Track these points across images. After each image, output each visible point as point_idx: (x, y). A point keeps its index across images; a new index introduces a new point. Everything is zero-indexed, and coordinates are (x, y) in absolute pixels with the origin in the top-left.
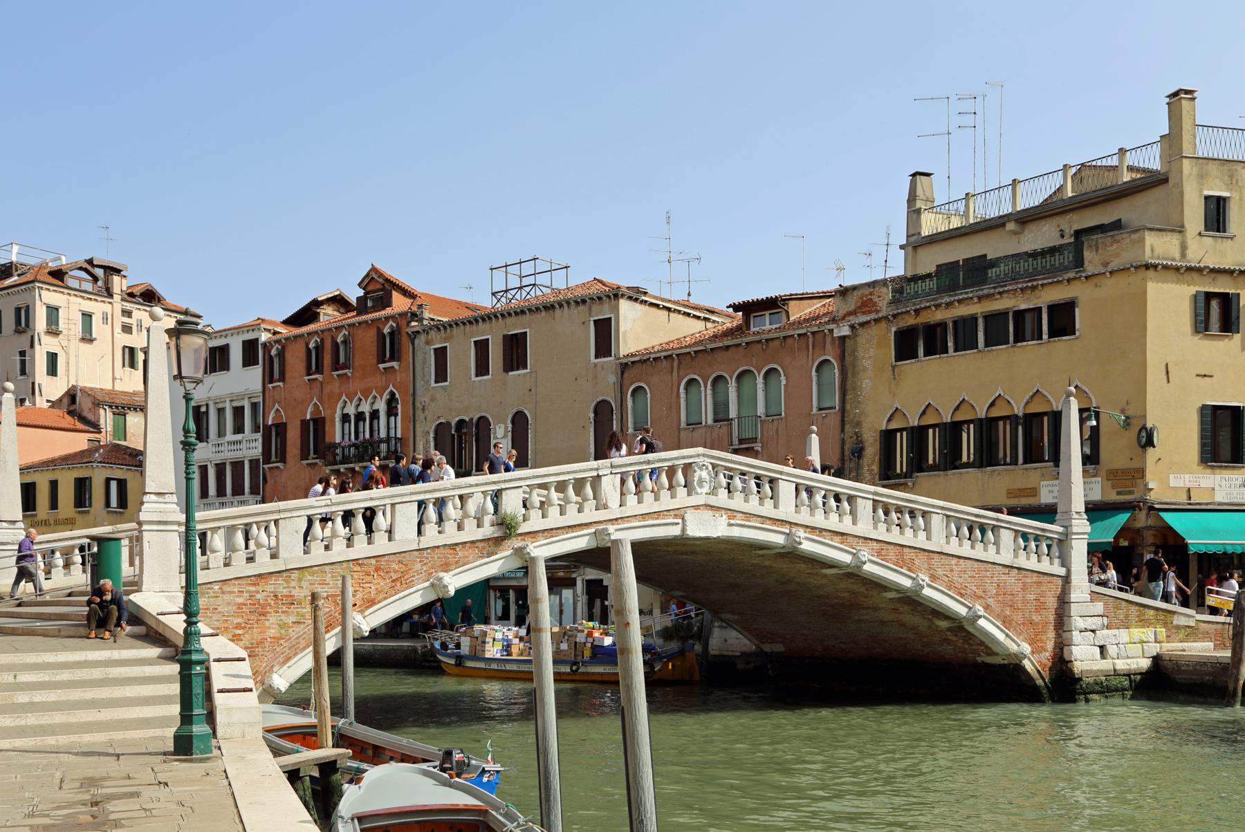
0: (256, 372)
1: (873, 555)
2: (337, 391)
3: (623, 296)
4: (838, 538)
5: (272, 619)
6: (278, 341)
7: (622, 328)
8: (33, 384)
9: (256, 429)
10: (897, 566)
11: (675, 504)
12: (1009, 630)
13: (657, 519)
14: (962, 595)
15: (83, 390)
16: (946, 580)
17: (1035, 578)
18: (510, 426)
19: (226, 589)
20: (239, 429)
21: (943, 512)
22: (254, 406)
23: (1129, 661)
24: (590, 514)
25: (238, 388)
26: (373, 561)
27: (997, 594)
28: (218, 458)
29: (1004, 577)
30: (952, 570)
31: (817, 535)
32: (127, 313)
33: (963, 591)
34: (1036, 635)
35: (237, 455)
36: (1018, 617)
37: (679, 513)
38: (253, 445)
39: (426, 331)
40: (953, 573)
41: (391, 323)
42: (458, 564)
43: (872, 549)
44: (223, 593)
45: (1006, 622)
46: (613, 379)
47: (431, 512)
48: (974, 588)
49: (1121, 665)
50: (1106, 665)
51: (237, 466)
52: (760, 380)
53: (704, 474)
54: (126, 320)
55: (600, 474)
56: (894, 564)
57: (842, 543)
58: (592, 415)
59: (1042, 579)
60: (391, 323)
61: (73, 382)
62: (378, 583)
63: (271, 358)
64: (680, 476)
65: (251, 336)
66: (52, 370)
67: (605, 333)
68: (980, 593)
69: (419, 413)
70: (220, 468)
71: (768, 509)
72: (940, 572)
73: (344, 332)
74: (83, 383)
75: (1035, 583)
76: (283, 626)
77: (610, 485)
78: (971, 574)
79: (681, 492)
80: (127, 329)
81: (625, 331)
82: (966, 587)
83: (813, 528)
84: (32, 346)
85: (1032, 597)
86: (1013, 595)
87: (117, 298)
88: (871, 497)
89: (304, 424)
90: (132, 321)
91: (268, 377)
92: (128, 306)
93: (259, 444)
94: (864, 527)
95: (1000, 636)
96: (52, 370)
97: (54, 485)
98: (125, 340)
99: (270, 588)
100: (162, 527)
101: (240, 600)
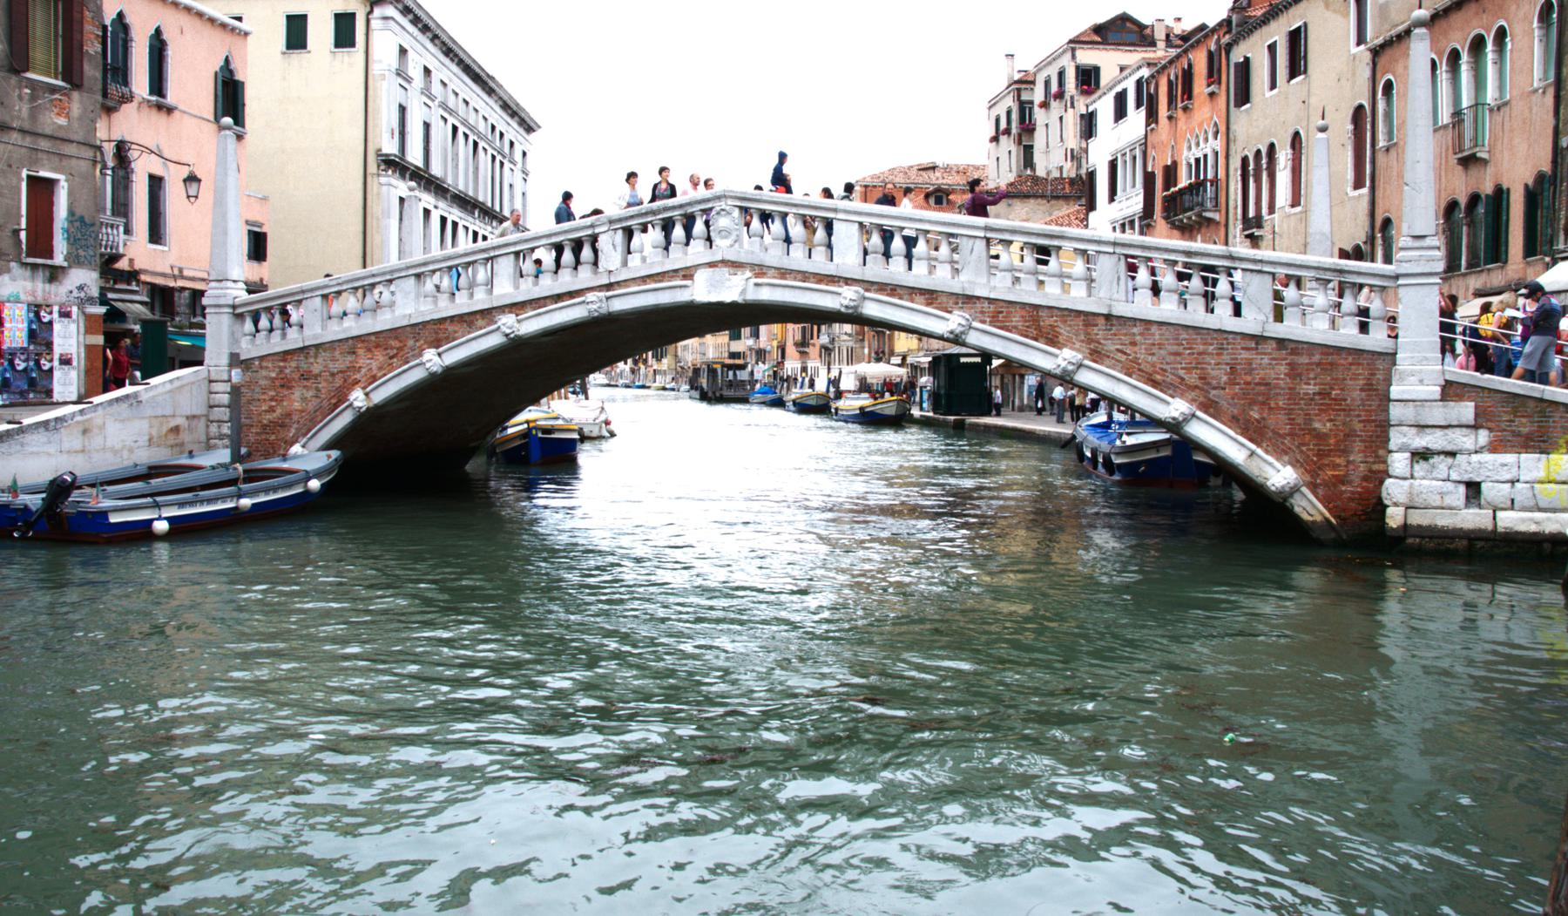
1: (983, 322)
4: (918, 298)
5: (297, 393)
10: (1027, 336)
12: (1259, 445)
13: (660, 281)
14: (1155, 384)
16: (1123, 358)
19: (264, 364)
21: (1119, 250)
23: (1538, 515)
24: (585, 277)
26: (373, 338)
27: (1232, 383)
29: (1245, 355)
30: (1134, 344)
31: (888, 295)
33: (1158, 377)
34: (1321, 454)
36: (1279, 421)
37: (687, 273)
40: (1136, 349)
42: (449, 339)
43: (982, 312)
44: (261, 368)
45: (1253, 432)
48: (1182, 373)
49: (1510, 520)
50: (1473, 519)
55: (597, 231)
56: (1022, 335)
57: (928, 304)
62: (368, 361)
64: (699, 227)
68: (1192, 379)
71: (819, 263)
72: (1110, 346)
75: (1318, 364)
76: (304, 399)
78: (1175, 348)
82: (1165, 370)
85: (1312, 389)
86: (1267, 384)
88: (981, 234)
99: (294, 364)
100: (217, 310)
101: (273, 375)
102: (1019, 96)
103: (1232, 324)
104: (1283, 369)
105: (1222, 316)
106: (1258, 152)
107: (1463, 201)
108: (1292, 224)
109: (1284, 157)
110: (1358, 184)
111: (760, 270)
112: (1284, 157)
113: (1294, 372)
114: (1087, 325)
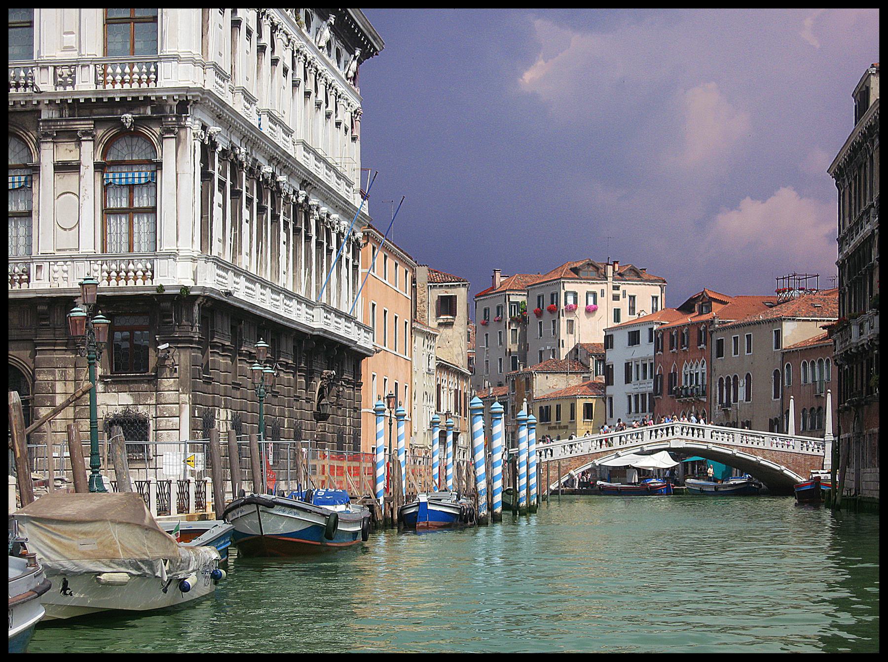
0: (653, 345)
2: (683, 359)
3: (784, 319)
6: (660, 330)
7: (784, 336)
8: (559, 340)
9: (651, 377)
11: (668, 438)
15: (582, 346)
17: (810, 457)
18: (745, 380)
20: (645, 378)
22: (651, 364)
24: (640, 442)
25: (644, 355)
27: (793, 462)
28: (635, 392)
32: (616, 288)
35: (644, 390)
37: (668, 441)
38: (650, 385)
39: (717, 330)
41: (703, 325)
45: (797, 472)
46: (780, 359)
47: (653, 433)
51: (644, 395)
52: (825, 363)
53: (678, 429)
54: (616, 292)
58: (773, 377)
59: (812, 457)
60: (703, 325)
61: (577, 342)
63: (658, 338)
65: (650, 326)
66: (571, 330)
67: (778, 334)
68: (785, 462)
69: (713, 371)
70: (637, 396)
71: (701, 438)
73: (686, 328)
74: (582, 342)
77: (647, 434)
79: (670, 434)
80: (616, 298)
81: (786, 336)
83: (717, 444)
84: (559, 317)
85: (809, 463)
87: (610, 279)
89: (670, 374)
90: (620, 292)
91: (657, 349)
92: (617, 283)
93: (652, 385)
94: (737, 442)
95: (794, 477)
96: (571, 330)
97: (558, 408)
98: (616, 304)
102: (509, 299)
103: (793, 451)
104: (803, 459)
105: (790, 449)
106: (728, 378)
107: (816, 408)
108: (746, 407)
109: (742, 383)
110: (776, 396)
111: (686, 440)
112: (742, 383)
113: (805, 460)
114: (763, 452)
